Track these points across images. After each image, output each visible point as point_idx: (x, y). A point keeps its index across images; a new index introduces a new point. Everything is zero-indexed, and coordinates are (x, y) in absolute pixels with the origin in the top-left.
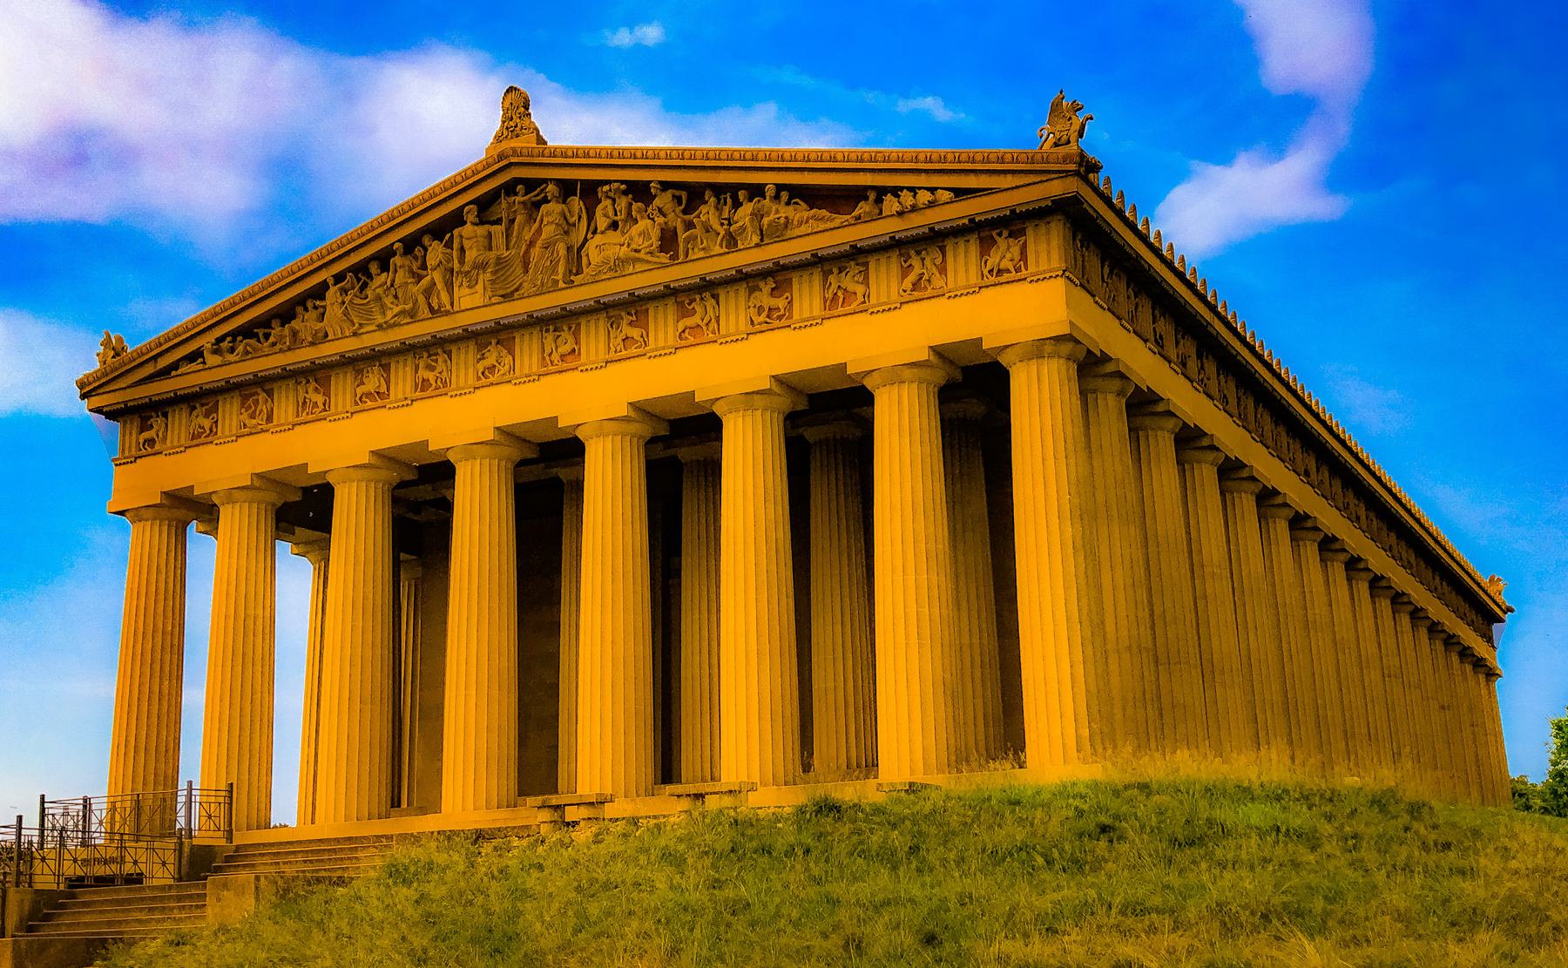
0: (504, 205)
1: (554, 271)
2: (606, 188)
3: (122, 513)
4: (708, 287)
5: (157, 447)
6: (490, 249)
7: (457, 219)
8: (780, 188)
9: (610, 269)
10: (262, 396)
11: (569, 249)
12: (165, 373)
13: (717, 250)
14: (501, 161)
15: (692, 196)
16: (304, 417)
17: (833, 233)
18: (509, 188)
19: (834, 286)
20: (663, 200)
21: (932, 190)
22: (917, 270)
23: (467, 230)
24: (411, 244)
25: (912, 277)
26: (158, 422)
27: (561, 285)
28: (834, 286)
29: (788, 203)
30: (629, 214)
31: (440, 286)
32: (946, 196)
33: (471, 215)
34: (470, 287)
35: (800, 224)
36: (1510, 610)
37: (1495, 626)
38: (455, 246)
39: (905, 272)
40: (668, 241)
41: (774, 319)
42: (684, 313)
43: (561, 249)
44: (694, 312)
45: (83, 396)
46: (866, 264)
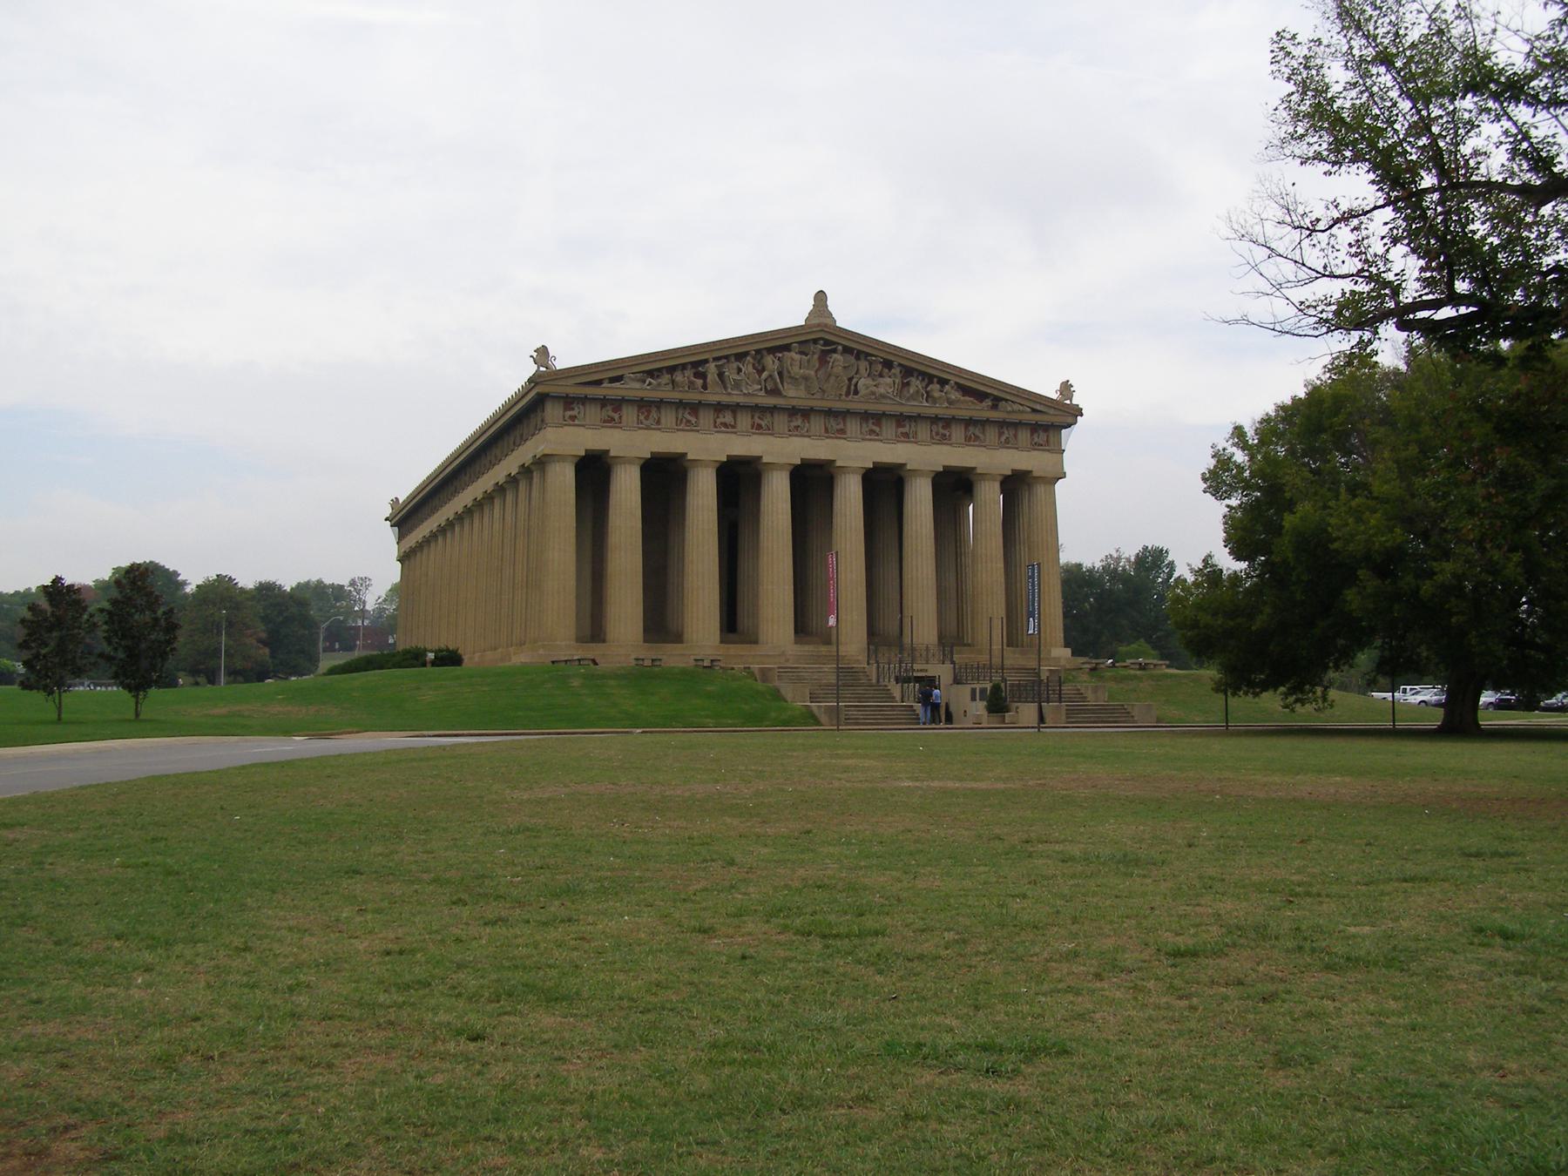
4: (917, 418)
10: (654, 410)
12: (599, 383)
15: (908, 372)
17: (982, 411)
18: (815, 341)
20: (896, 371)
23: (793, 354)
24: (758, 352)
39: (1001, 434)
41: (944, 440)
42: (899, 425)
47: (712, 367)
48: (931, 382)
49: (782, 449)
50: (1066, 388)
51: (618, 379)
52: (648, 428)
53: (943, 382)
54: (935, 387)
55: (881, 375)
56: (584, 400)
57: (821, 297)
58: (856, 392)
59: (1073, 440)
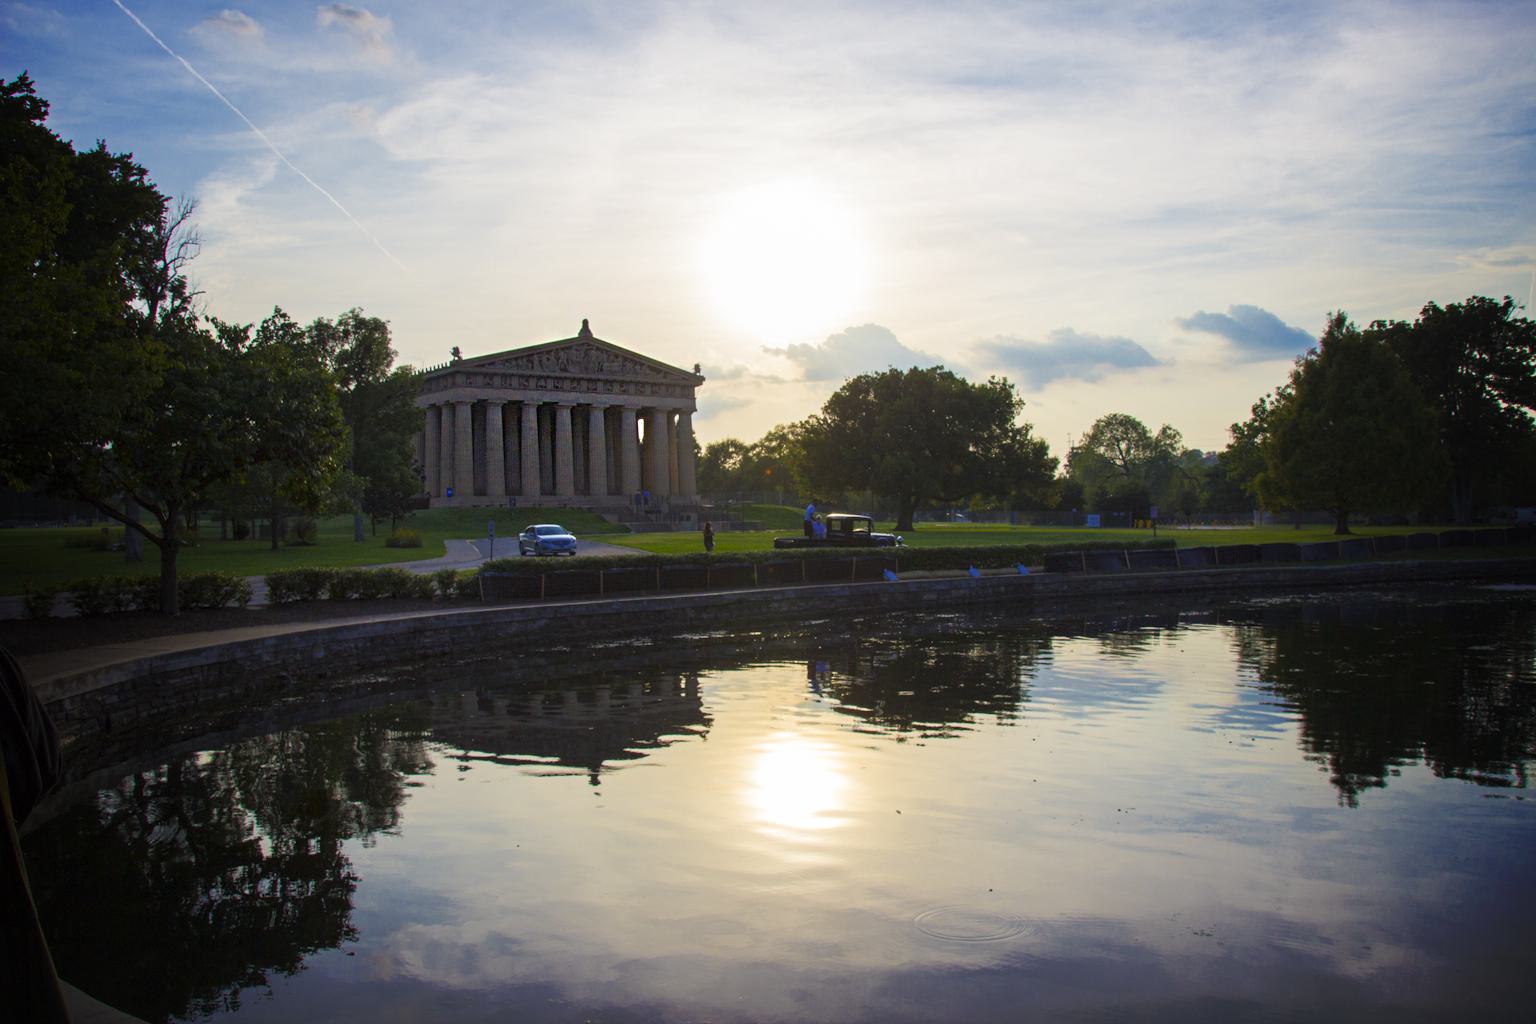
12: (483, 366)
18: (583, 344)
20: (620, 359)
24: (557, 349)
41: (642, 393)
42: (621, 386)
47: (536, 358)
48: (636, 365)
49: (569, 398)
50: (697, 368)
51: (493, 363)
52: (506, 388)
53: (642, 365)
54: (638, 367)
55: (613, 361)
56: (476, 374)
57: (585, 323)
58: (602, 370)
59: (701, 393)
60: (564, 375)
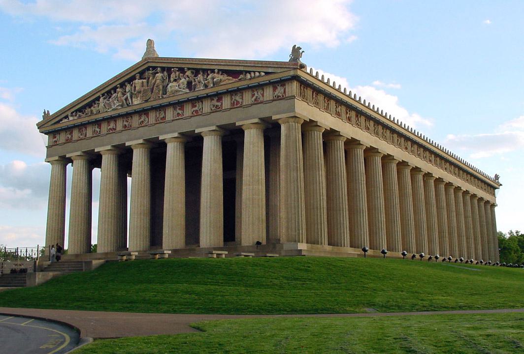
0: (147, 74)
1: (159, 94)
2: (173, 69)
3: (48, 162)
5: (57, 143)
6: (143, 86)
7: (133, 78)
8: (219, 70)
9: (173, 94)
10: (84, 129)
11: (163, 87)
12: (58, 122)
13: (202, 88)
14: (145, 61)
15: (196, 72)
16: (94, 135)
18: (148, 69)
19: (233, 100)
20: (189, 73)
21: (259, 72)
22: (256, 95)
25: (254, 98)
26: (58, 136)
27: (161, 97)
28: (233, 100)
29: (221, 75)
30: (179, 77)
31: (129, 98)
32: (263, 74)
33: (138, 76)
34: (137, 98)
35: (224, 81)
36: (501, 185)
37: (496, 190)
38: (133, 85)
40: (189, 85)
41: (217, 109)
43: (161, 87)
44: (196, 106)
45: (38, 128)
46: (242, 93)
57: (150, 43)
60: (128, 110)
